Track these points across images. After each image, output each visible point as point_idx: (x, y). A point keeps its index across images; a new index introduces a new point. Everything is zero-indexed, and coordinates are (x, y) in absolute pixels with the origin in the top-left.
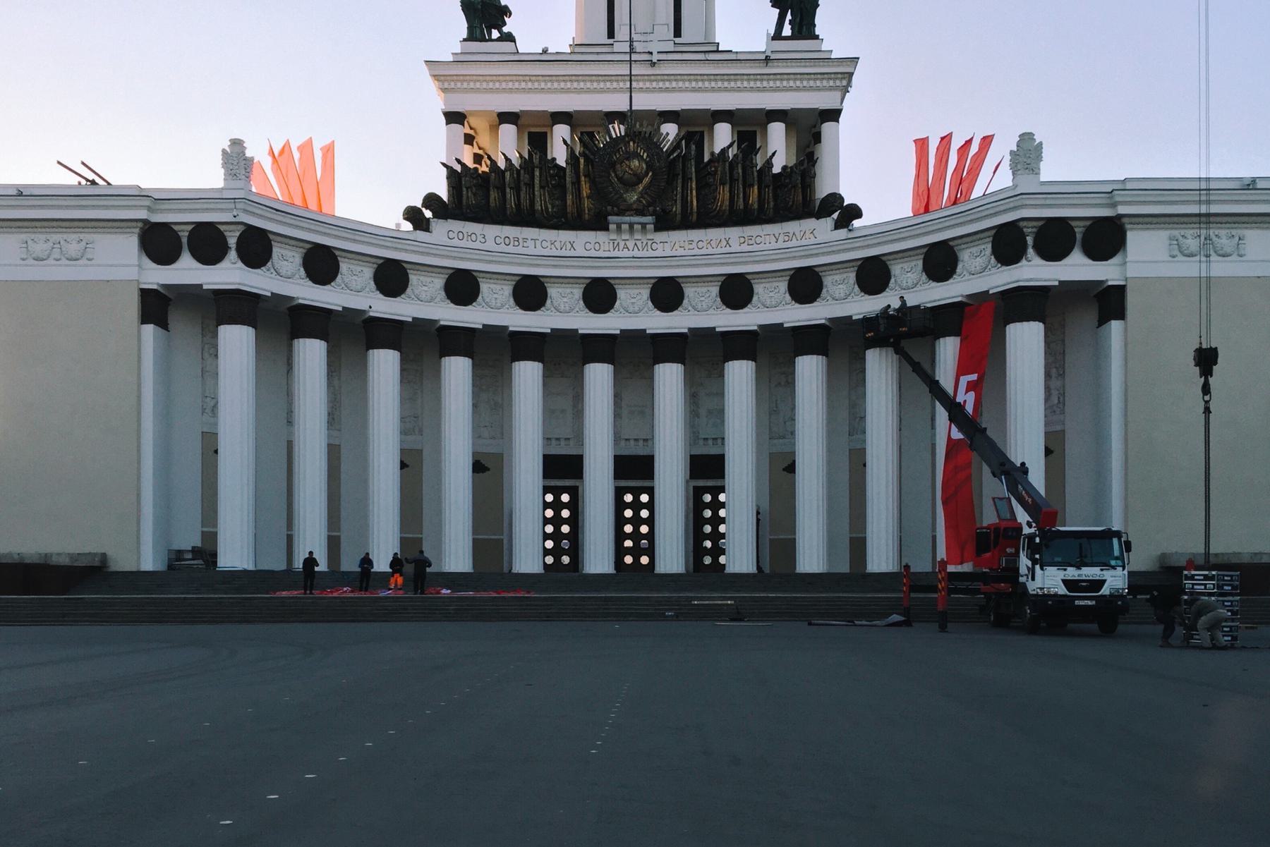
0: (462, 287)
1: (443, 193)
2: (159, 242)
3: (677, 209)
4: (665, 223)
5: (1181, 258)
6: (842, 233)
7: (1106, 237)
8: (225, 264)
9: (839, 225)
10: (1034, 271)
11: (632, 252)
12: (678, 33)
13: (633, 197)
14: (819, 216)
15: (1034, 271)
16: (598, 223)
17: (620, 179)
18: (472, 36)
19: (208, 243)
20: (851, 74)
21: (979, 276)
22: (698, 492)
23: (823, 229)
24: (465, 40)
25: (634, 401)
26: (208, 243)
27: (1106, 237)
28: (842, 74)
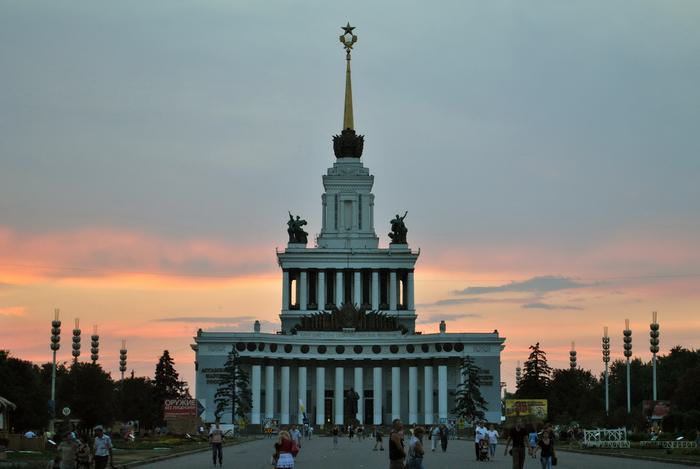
0: (305, 349)
1: (300, 323)
2: (240, 346)
3: (360, 325)
4: (357, 330)
6: (403, 337)
7: (459, 347)
9: (403, 333)
10: (444, 354)
11: (349, 337)
12: (360, 228)
13: (349, 324)
14: (397, 330)
15: (444, 354)
16: (340, 329)
18: (291, 241)
19: (252, 347)
21: (432, 354)
22: (366, 401)
23: (398, 334)
25: (349, 377)
26: (252, 347)
27: (459, 347)
28: (413, 258)
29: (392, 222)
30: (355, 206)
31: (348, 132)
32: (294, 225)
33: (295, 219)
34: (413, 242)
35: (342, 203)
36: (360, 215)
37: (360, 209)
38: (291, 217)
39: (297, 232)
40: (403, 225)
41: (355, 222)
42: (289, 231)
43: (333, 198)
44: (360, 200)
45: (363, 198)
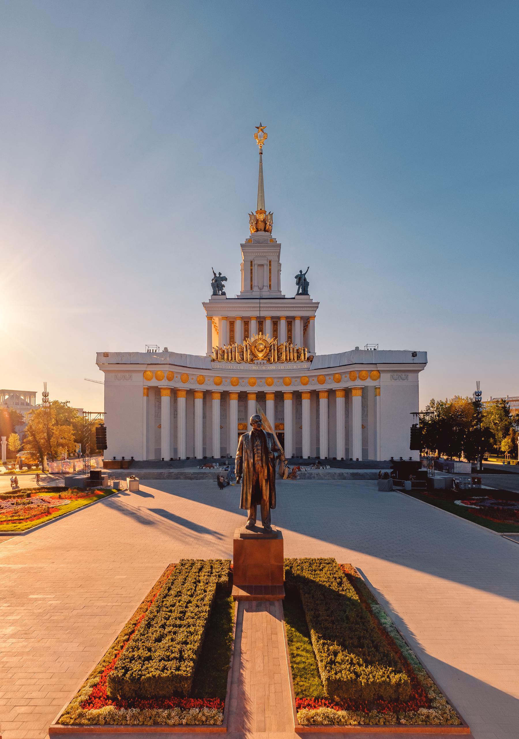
5: (393, 380)
8: (163, 381)
13: (260, 355)
15: (359, 383)
17: (258, 350)
18: (215, 294)
20: (318, 307)
24: (213, 295)
28: (316, 306)
29: (296, 277)
30: (266, 268)
31: (262, 211)
32: (216, 281)
33: (218, 275)
34: (314, 294)
35: (256, 266)
36: (270, 277)
37: (270, 272)
38: (215, 274)
39: (218, 283)
40: (305, 280)
41: (266, 283)
42: (213, 285)
43: (250, 263)
44: (270, 265)
45: (272, 263)
